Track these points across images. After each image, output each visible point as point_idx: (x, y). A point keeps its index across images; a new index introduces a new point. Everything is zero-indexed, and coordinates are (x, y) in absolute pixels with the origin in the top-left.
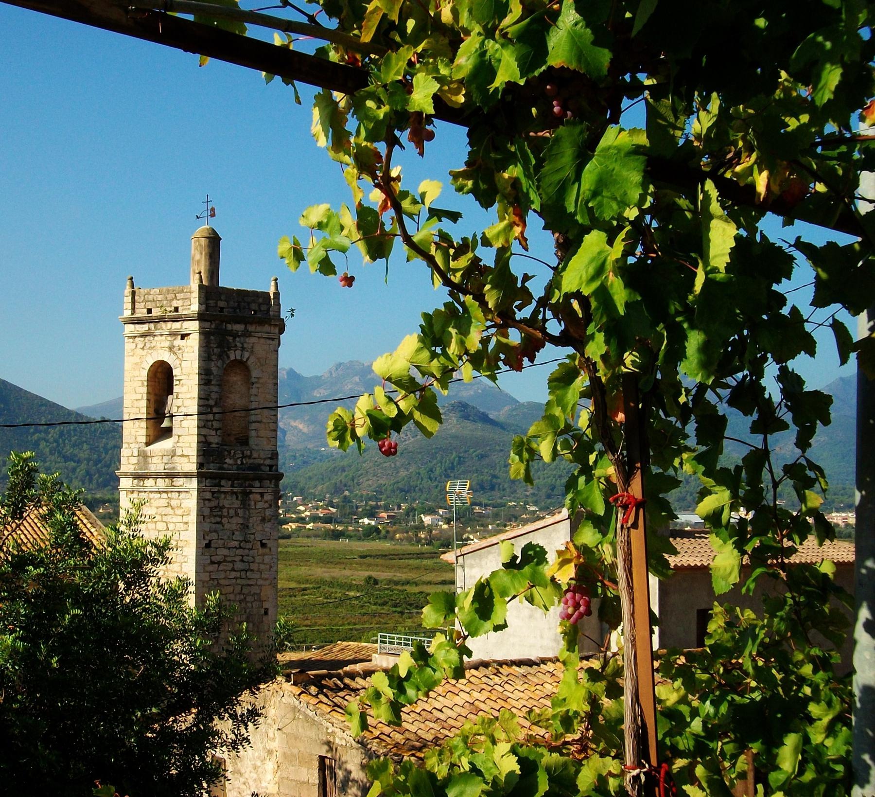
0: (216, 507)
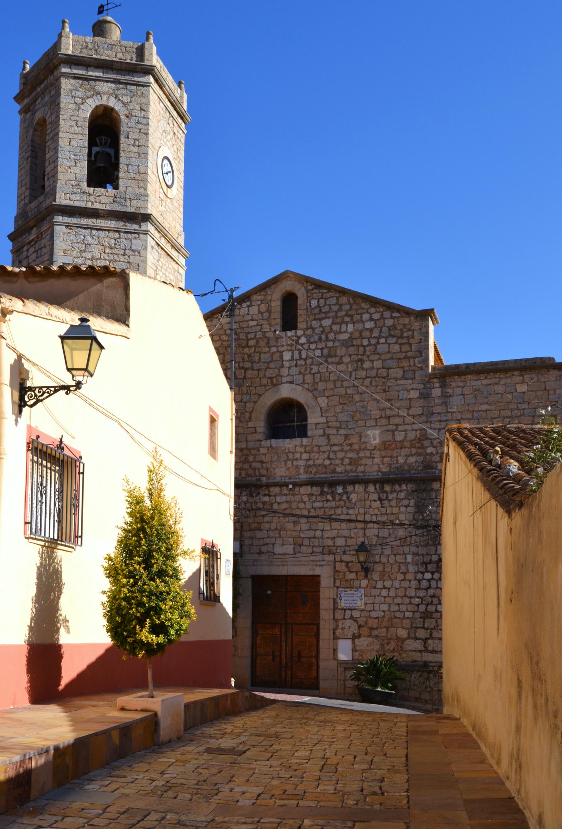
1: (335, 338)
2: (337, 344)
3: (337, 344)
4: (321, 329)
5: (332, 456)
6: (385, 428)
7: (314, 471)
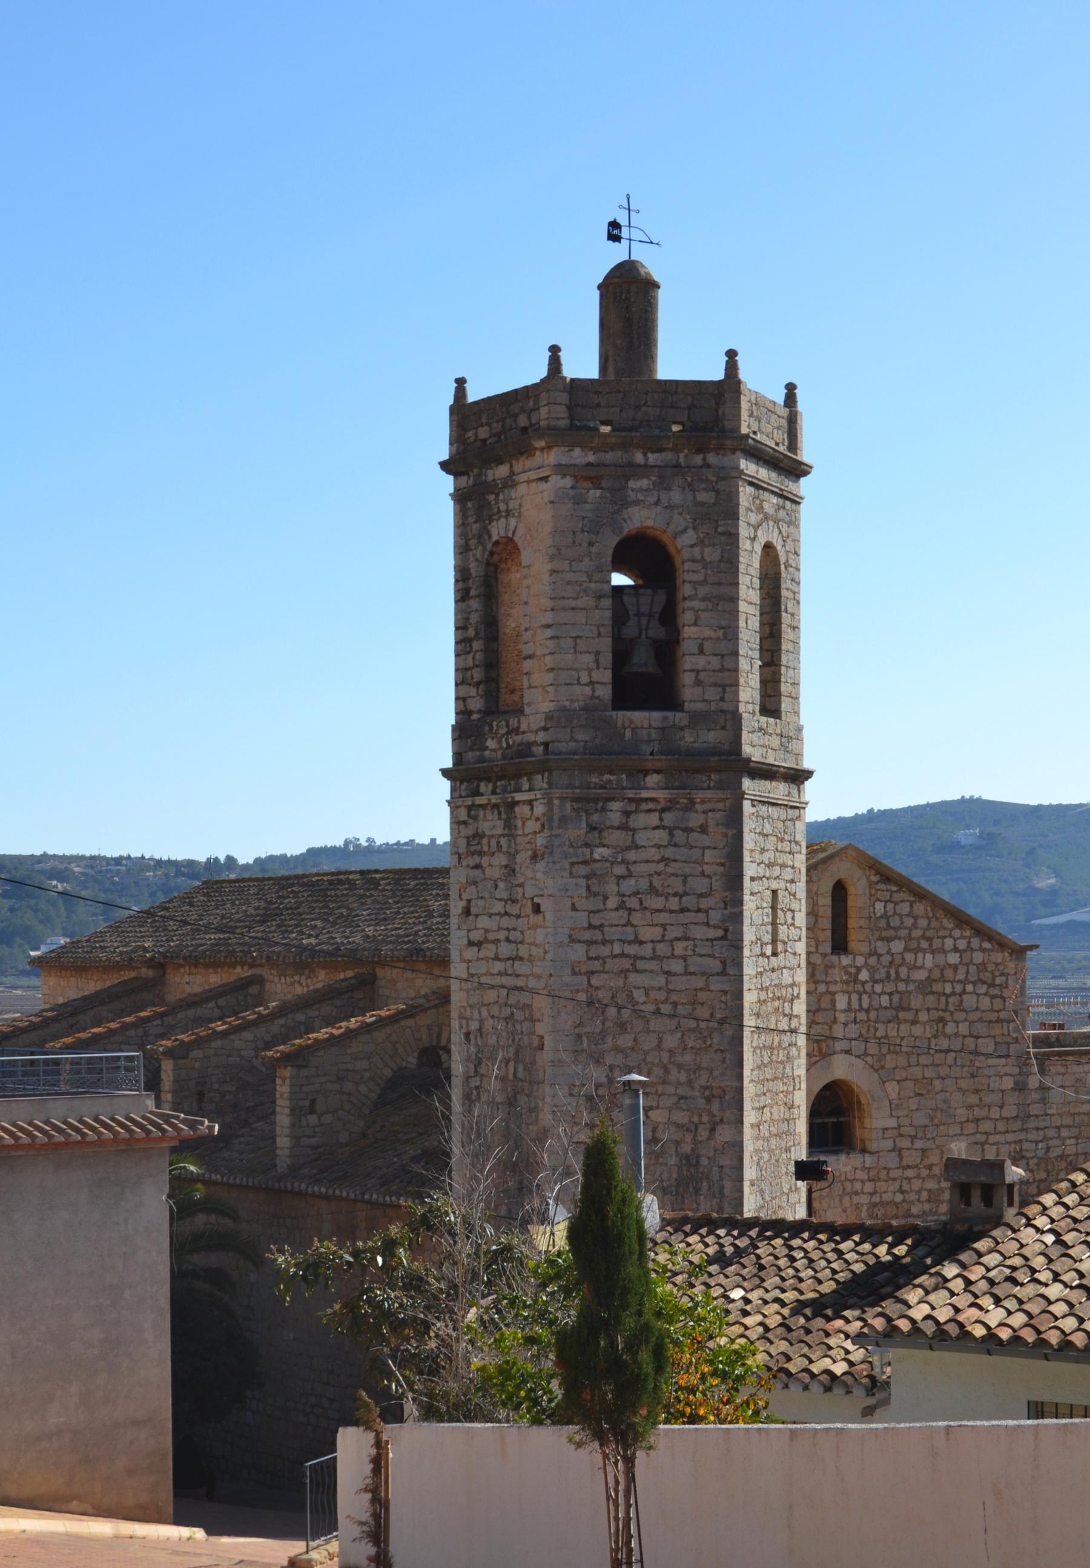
0: (474, 836)
1: (908, 976)
2: (911, 987)
3: (911, 987)
4: (889, 958)
5: (905, 1187)
6: (972, 1139)
7: (880, 1212)
